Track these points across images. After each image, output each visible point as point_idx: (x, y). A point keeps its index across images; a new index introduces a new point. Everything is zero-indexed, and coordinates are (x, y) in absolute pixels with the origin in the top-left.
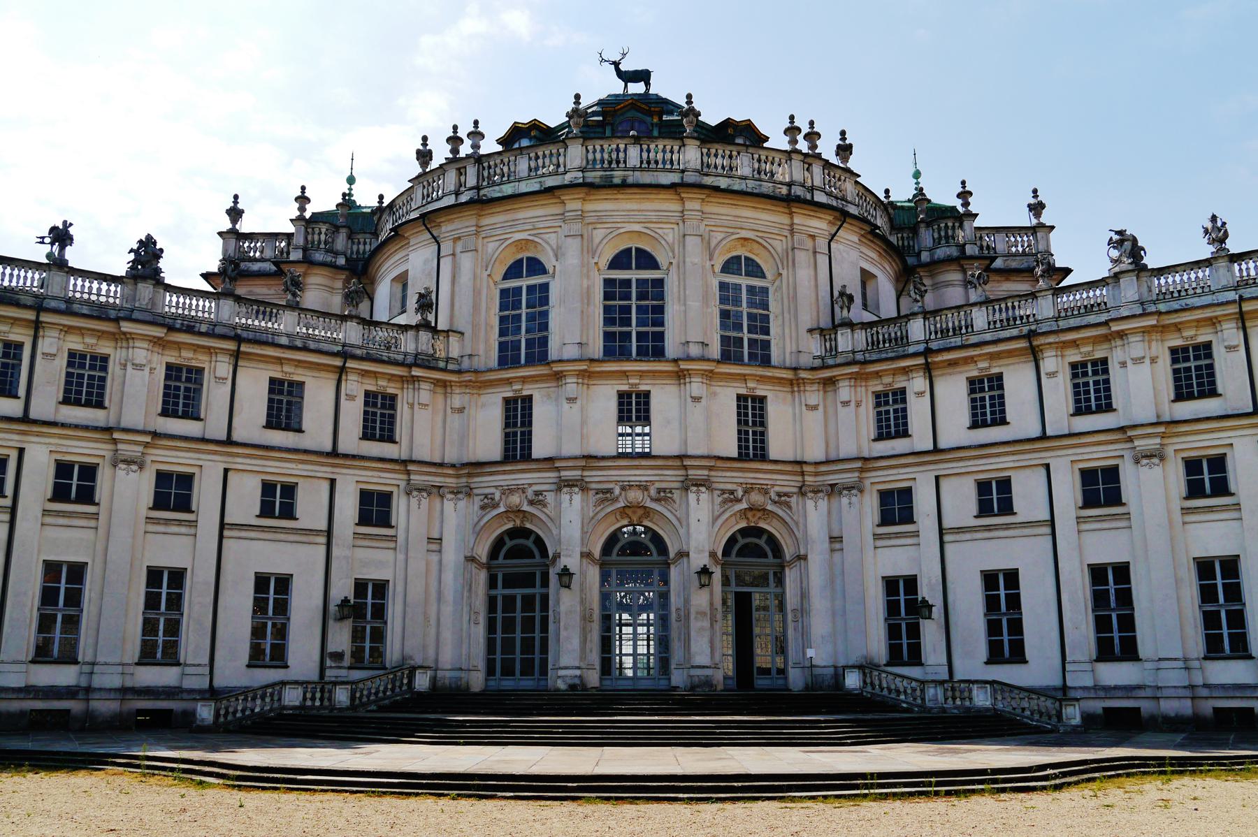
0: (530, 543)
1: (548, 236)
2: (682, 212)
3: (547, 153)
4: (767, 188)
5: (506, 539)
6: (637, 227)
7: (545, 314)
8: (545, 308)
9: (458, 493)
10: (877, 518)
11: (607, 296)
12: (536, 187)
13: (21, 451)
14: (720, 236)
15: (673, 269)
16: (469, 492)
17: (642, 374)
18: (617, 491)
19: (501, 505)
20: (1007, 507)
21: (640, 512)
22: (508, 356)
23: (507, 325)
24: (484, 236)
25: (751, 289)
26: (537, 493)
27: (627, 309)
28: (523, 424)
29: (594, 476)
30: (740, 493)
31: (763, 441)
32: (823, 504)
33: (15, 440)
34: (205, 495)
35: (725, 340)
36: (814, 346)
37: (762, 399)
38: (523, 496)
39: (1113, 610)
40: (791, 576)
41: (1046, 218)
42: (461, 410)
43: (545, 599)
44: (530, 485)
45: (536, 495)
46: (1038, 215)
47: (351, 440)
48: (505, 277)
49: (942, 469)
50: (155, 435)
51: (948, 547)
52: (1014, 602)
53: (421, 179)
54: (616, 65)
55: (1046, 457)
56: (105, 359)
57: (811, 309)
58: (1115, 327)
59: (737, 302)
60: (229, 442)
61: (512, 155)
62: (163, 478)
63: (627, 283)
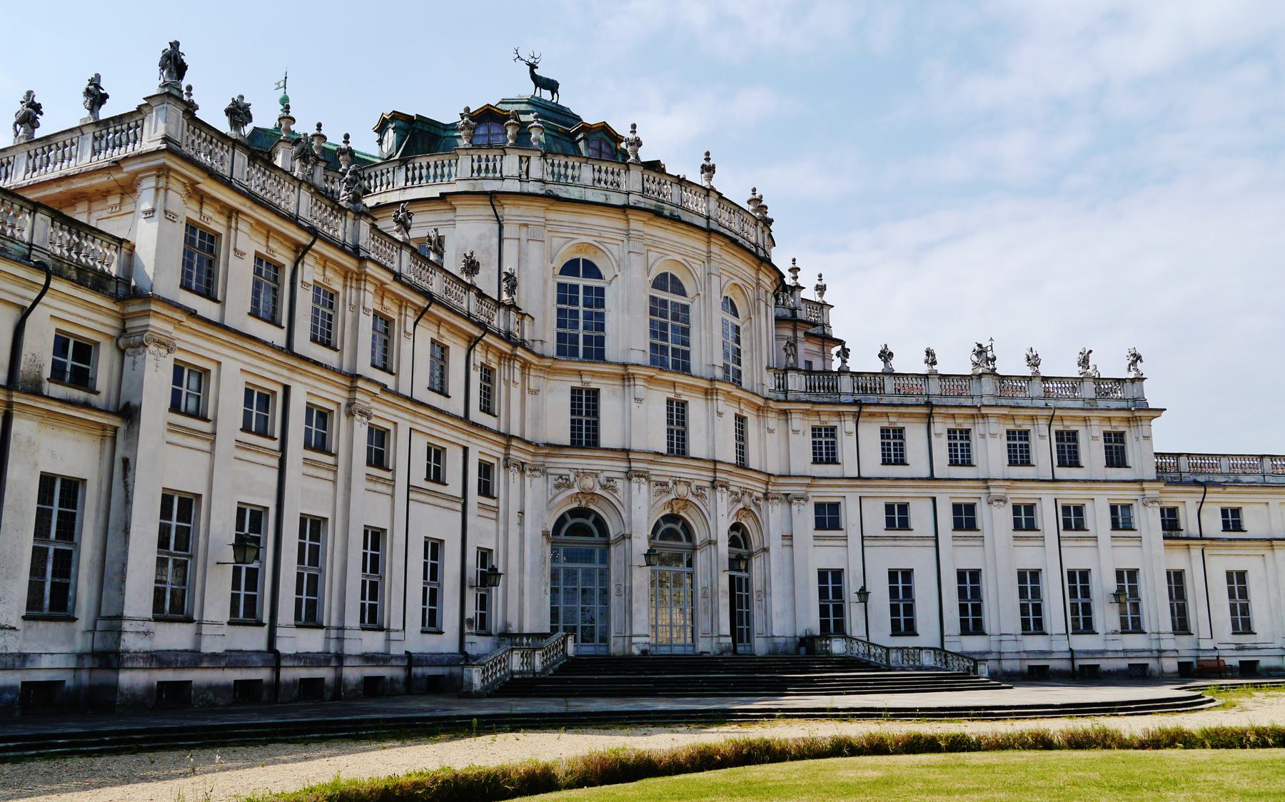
1: (611, 246)
3: (610, 169)
5: (568, 517)
6: (679, 258)
7: (601, 316)
8: (601, 310)
9: (535, 470)
12: (601, 199)
13: (287, 389)
16: (542, 470)
17: (685, 386)
18: (671, 484)
19: (575, 485)
20: (905, 525)
21: (682, 504)
22: (566, 347)
23: (564, 319)
24: (550, 229)
27: (664, 326)
29: (656, 470)
33: (284, 376)
38: (596, 480)
39: (969, 601)
40: (756, 563)
41: (827, 298)
42: (535, 392)
44: (602, 471)
45: (608, 481)
46: (821, 295)
48: (563, 272)
49: (865, 492)
52: (908, 591)
53: (471, 152)
54: (533, 67)
55: (934, 493)
58: (984, 411)
60: (410, 399)
61: (578, 161)
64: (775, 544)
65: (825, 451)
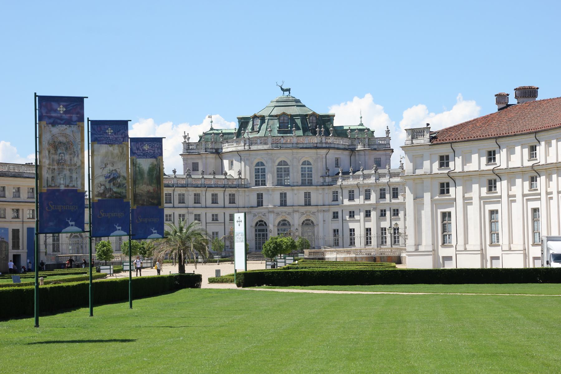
0: (263, 223)
2: (293, 153)
4: (311, 145)
10: (332, 217)
11: (278, 171)
13: (174, 213)
14: (301, 158)
15: (291, 166)
17: (284, 189)
23: (257, 176)
25: (308, 168)
26: (265, 214)
27: (282, 174)
28: (261, 199)
30: (305, 213)
31: (310, 201)
32: (322, 214)
34: (203, 218)
35: (302, 180)
36: (321, 180)
37: (310, 193)
42: (248, 196)
43: (267, 234)
47: (227, 204)
48: (256, 166)
50: (195, 207)
51: (344, 224)
56: (184, 194)
57: (321, 172)
59: (305, 171)
62: (195, 215)
63: (282, 168)
65: (336, 199)
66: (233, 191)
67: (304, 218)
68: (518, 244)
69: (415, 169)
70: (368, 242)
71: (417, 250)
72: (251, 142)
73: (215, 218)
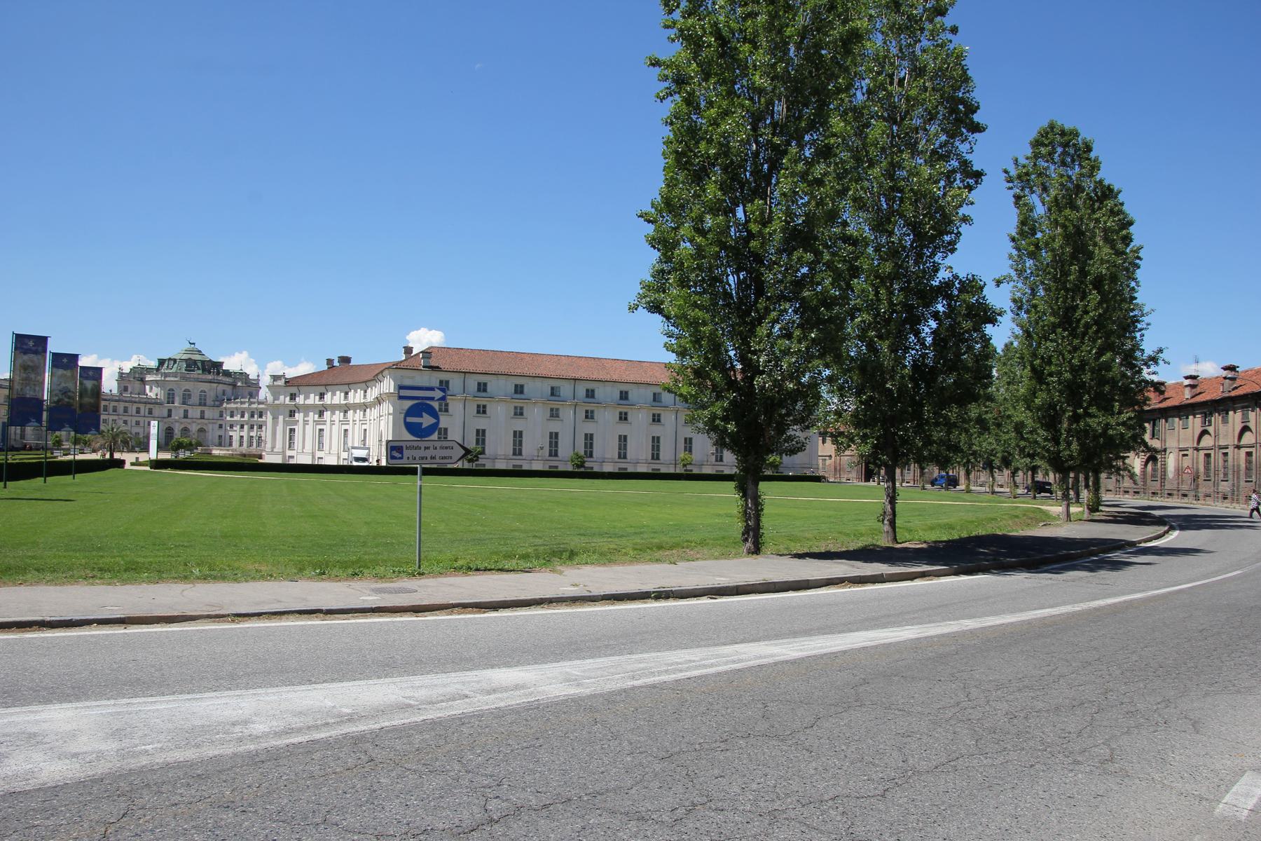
23: (168, 398)
34: (129, 423)
64: (211, 431)
65: (221, 416)
66: (151, 406)
67: (199, 427)
68: (334, 450)
69: (274, 400)
70: (241, 444)
71: (272, 451)
72: (166, 375)
73: (138, 423)
